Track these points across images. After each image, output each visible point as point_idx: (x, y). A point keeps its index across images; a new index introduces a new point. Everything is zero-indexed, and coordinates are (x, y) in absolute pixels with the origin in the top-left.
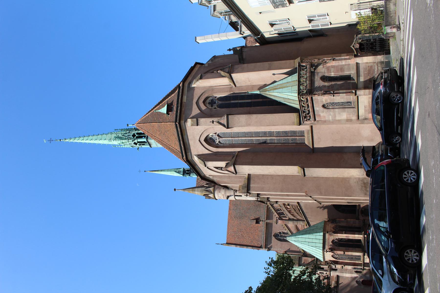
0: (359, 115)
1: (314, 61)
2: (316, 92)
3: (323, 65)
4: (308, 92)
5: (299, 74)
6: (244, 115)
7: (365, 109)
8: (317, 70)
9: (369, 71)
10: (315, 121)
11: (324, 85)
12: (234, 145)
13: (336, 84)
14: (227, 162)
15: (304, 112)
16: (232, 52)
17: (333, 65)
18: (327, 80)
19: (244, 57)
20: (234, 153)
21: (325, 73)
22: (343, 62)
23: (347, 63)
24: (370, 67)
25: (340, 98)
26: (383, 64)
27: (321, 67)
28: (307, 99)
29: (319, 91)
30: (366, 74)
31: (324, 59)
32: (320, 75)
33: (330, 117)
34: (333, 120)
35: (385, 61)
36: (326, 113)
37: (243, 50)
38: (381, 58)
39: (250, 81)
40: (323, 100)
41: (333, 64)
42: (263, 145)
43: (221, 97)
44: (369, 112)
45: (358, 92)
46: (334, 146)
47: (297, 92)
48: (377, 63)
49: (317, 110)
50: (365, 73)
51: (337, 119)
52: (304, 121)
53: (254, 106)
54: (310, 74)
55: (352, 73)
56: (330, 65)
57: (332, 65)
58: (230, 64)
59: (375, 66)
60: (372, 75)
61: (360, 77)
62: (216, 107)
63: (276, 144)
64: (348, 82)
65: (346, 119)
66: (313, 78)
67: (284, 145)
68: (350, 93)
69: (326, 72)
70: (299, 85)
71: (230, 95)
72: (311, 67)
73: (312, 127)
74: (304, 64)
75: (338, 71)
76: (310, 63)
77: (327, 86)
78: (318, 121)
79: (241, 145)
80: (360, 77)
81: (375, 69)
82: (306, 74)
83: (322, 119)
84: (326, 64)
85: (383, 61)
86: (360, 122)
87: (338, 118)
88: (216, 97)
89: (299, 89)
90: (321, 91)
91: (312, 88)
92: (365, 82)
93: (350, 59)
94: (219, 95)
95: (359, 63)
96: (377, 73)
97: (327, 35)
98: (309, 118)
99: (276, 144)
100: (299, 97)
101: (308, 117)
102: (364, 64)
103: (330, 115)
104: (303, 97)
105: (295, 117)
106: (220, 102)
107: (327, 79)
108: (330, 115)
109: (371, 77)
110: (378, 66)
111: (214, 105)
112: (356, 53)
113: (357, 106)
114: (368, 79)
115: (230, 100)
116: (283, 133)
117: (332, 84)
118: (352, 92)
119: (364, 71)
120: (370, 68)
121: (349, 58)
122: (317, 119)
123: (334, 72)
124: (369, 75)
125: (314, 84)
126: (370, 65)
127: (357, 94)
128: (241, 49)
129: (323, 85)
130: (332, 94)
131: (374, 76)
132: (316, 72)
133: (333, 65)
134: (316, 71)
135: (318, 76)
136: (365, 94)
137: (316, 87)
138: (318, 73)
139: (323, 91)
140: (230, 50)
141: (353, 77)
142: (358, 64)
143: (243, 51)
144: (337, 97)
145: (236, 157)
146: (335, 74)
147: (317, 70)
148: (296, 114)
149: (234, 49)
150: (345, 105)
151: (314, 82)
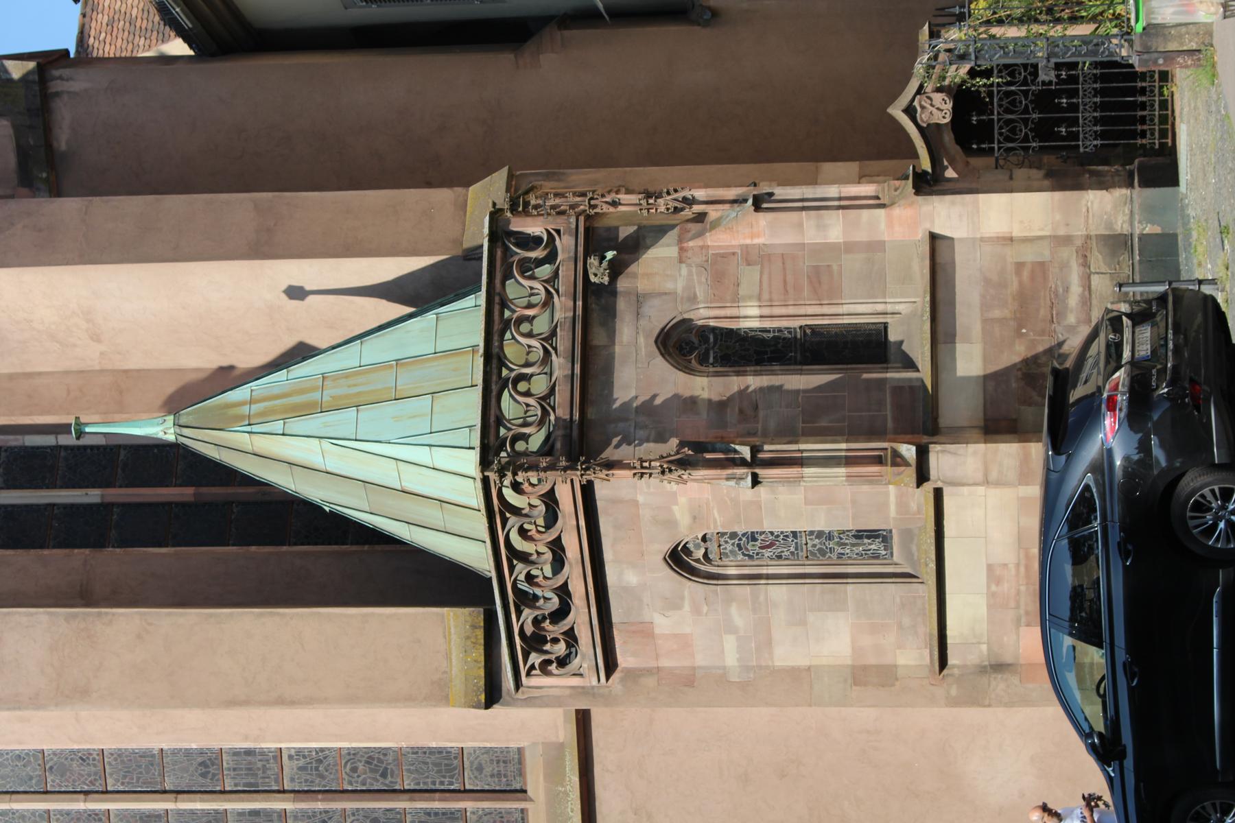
0: (949, 633)
1: (614, 204)
2: (624, 446)
3: (681, 240)
4: (558, 445)
5: (497, 299)
6: (41, 616)
7: (994, 588)
8: (635, 276)
9: (1024, 300)
10: (608, 678)
11: (687, 394)
15: (525, 600)
17: (759, 246)
18: (711, 360)
19: (62, 139)
21: (693, 299)
23: (861, 236)
24: (1033, 271)
25: (807, 502)
26: (1125, 257)
27: (661, 253)
28: (550, 499)
29: (648, 441)
30: (1002, 321)
31: (687, 193)
32: (659, 316)
33: (730, 643)
35: (1142, 237)
36: (696, 611)
37: (56, 86)
38: (1109, 207)
39: (96, 338)
40: (675, 508)
41: (758, 236)
44: (1022, 612)
45: (943, 460)
47: (476, 442)
48: (1079, 243)
49: (627, 590)
50: (997, 313)
51: (778, 663)
52: (523, 673)
53: (124, 543)
54: (580, 303)
55: (898, 308)
56: (734, 243)
57: (748, 241)
59: (1064, 266)
60: (1042, 333)
61: (953, 342)
64: (865, 376)
65: (849, 662)
66: (599, 338)
68: (879, 461)
69: (700, 294)
70: (495, 388)
72: (587, 255)
73: (583, 720)
74: (534, 227)
76: (582, 219)
77: (710, 401)
78: (634, 675)
80: (958, 345)
81: (1067, 289)
82: (548, 303)
83: (665, 663)
84: (700, 234)
85: (1126, 229)
86: (954, 691)
87: (786, 655)
89: (492, 419)
90: (661, 438)
91: (591, 413)
92: (993, 381)
93: (883, 206)
95: (953, 239)
96: (1079, 322)
97: (715, 13)
98: (561, 649)
100: (486, 482)
101: (555, 641)
103: (732, 630)
104: (519, 479)
105: (455, 638)
108: (732, 630)
109: (1040, 349)
110: (1085, 264)
112: (926, 164)
113: (933, 566)
114: (1015, 358)
116: (354, 770)
117: (742, 393)
118: (897, 460)
119: (983, 297)
120: (1032, 278)
121: (877, 198)
122: (624, 659)
123: (766, 296)
124: (1020, 335)
125: (609, 384)
126: (1029, 255)
127: (933, 473)
128: (36, 77)
129: (676, 396)
130: (743, 463)
131: (1060, 344)
132: (628, 293)
133: (756, 241)
134: (622, 284)
136: (994, 475)
137: (626, 405)
138: (639, 300)
141: (901, 342)
142: (939, 243)
143: (57, 94)
144: (781, 489)
146: (766, 311)
147: (635, 276)
148: (467, 611)
150: (840, 555)
151: (608, 370)
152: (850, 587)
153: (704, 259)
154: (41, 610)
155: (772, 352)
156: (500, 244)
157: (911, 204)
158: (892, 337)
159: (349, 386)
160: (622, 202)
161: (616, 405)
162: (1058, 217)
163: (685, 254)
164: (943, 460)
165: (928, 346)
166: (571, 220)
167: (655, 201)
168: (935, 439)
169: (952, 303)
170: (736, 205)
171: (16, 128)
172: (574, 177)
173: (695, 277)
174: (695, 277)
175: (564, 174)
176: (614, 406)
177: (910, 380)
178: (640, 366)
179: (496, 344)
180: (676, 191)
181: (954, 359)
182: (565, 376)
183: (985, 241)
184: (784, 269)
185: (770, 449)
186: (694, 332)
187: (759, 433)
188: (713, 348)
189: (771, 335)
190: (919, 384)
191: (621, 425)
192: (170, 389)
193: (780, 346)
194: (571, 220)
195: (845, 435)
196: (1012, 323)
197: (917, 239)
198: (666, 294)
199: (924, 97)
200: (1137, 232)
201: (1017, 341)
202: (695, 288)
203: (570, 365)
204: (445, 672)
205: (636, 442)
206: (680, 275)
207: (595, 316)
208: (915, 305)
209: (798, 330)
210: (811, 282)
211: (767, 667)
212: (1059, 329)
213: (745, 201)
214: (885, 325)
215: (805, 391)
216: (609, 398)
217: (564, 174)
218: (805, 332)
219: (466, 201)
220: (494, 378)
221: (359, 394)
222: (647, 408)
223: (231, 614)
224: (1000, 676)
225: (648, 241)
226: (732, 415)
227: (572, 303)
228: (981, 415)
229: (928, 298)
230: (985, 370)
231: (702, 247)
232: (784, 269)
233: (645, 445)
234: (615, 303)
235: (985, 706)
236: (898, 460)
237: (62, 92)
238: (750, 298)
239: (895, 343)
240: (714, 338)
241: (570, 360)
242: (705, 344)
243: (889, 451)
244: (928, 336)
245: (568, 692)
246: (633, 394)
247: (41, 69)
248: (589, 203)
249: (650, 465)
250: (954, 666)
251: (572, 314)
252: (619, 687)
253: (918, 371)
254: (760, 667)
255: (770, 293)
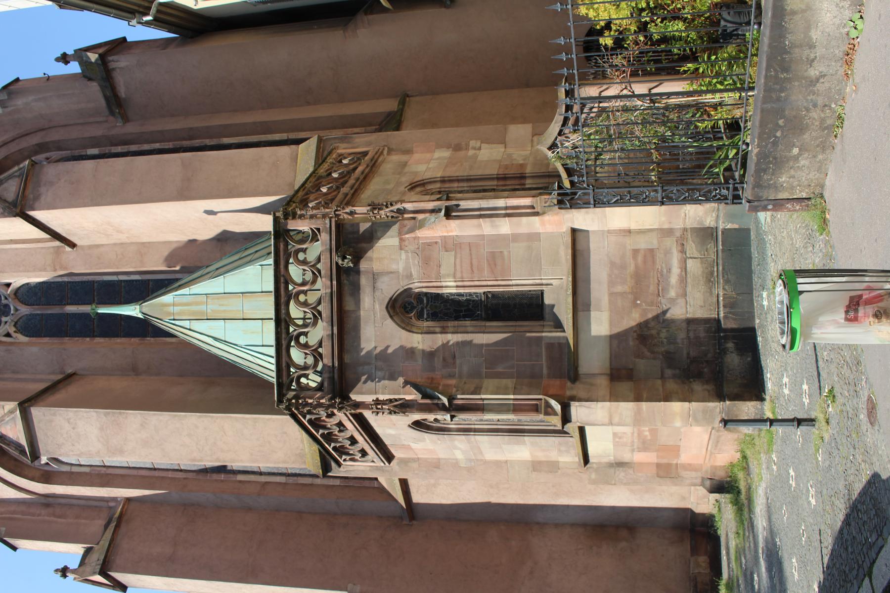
3: (400, 233)
5: (282, 280)
8: (371, 259)
9: (639, 278)
11: (409, 346)
12: (110, 471)
13: (469, 343)
14: (85, 546)
16: (74, 68)
18: (425, 316)
19: (122, 92)
20: (112, 504)
21: (410, 276)
22: (505, 227)
24: (645, 256)
26: (711, 246)
27: (388, 242)
29: (384, 379)
30: (622, 294)
32: (389, 288)
34: (471, 460)
35: (725, 231)
37: (112, 65)
38: (701, 214)
42: (216, 480)
43: (28, 284)
44: (635, 447)
46: (494, 500)
48: (678, 234)
50: (619, 289)
54: (335, 283)
57: (446, 234)
58: (24, 160)
59: (668, 252)
60: (652, 304)
61: (589, 310)
62: (12, 330)
63: (263, 479)
66: (349, 305)
67: (297, 484)
70: (284, 343)
71: (60, 280)
74: (303, 226)
75: (476, 271)
77: (423, 351)
79: (135, 472)
81: (669, 271)
84: (412, 230)
85: (713, 224)
86: (593, 476)
88: (8, 285)
89: (284, 365)
91: (347, 359)
92: (617, 339)
93: (537, 214)
94: (18, 281)
95: (588, 231)
96: (678, 296)
99: (263, 479)
102: (613, 238)
103: (456, 448)
106: (24, 310)
107: (422, 309)
109: (650, 316)
110: (683, 251)
111: (4, 319)
114: (633, 323)
115: (62, 302)
117: (445, 346)
118: (549, 410)
119: (610, 276)
120: (645, 262)
121: (533, 207)
124: (636, 305)
125: (357, 338)
126: (643, 243)
128: (100, 62)
129: (402, 347)
131: (665, 312)
132: (367, 272)
133: (450, 234)
134: (363, 265)
135: (378, 294)
136: (616, 420)
137: (369, 353)
138: (375, 277)
139: (401, 380)
140: (64, 59)
141: (553, 306)
142: (578, 234)
143: (114, 69)
145: (117, 527)
149: (80, 54)
151: (357, 328)
152: (525, 438)
153: (417, 247)
154: (92, 410)
155: (465, 311)
156: (282, 239)
157: (557, 214)
158: (547, 301)
159: (220, 305)
160: (357, 212)
161: (363, 353)
162: (663, 219)
163: (403, 243)
164: (578, 411)
165: (571, 315)
166: (327, 222)
167: (378, 212)
168: (578, 389)
169: (588, 281)
170: (433, 214)
171: (101, 86)
172: (357, 140)
173: (411, 261)
174: (411, 261)
175: (351, 137)
176: (362, 354)
177: (559, 338)
178: (377, 325)
179: (283, 311)
180: (392, 205)
181: (589, 324)
182: (328, 335)
183: (611, 233)
184: (471, 254)
185: (461, 398)
186: (413, 297)
187: (457, 375)
188: (426, 307)
189: (465, 298)
190: (564, 341)
191: (366, 367)
192: (166, 253)
193: (471, 306)
194: (327, 222)
195: (514, 378)
196: (630, 296)
197: (562, 231)
198: (391, 273)
199: (563, 138)
200: (721, 227)
201: (634, 310)
202: (411, 268)
203: (330, 328)
204: (302, 450)
205: (377, 380)
206: (401, 259)
207: (347, 289)
208: (562, 280)
209: (483, 295)
210: (489, 264)
211: (482, 460)
212: (663, 301)
213: (440, 210)
214: (542, 292)
215: (487, 345)
216: (358, 348)
217: (351, 137)
218: (487, 296)
219: (297, 155)
220: (284, 336)
221: (225, 311)
222: (383, 356)
223: (186, 415)
224: (621, 469)
225: (379, 234)
226: (438, 362)
227: (329, 283)
228: (608, 365)
229: (570, 279)
230: (611, 331)
231: (415, 238)
232: (471, 254)
233: (383, 381)
234: (359, 280)
235: (612, 484)
236: (549, 409)
237: (116, 68)
238: (448, 276)
239: (549, 305)
240: (426, 300)
241: (330, 323)
242: (421, 305)
243: (543, 401)
244: (571, 307)
245: (368, 468)
246: (373, 346)
247: (102, 57)
248: (335, 213)
249: (382, 407)
250: (593, 463)
251: (330, 290)
252: (397, 467)
253: (564, 331)
254: (477, 460)
255: (462, 272)
